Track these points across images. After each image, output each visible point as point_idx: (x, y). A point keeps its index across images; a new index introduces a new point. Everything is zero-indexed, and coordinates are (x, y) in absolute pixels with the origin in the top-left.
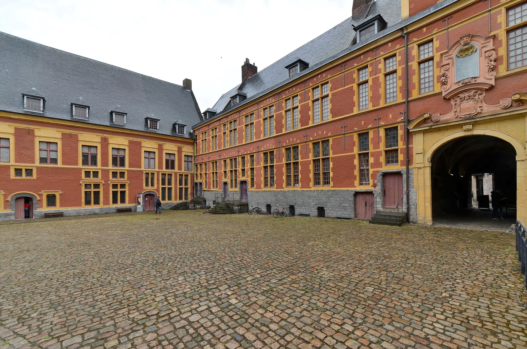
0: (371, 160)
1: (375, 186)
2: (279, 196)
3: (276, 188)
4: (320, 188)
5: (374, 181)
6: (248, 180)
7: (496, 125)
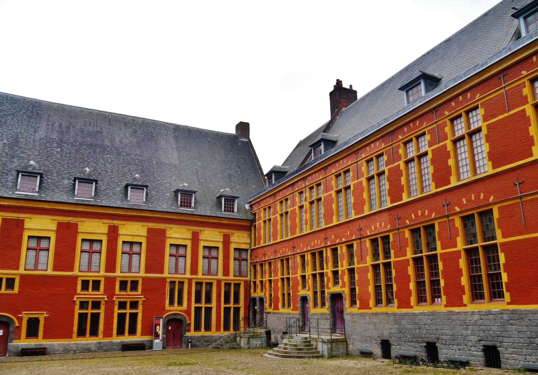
2: (403, 322)
4: (485, 306)
6: (344, 291)
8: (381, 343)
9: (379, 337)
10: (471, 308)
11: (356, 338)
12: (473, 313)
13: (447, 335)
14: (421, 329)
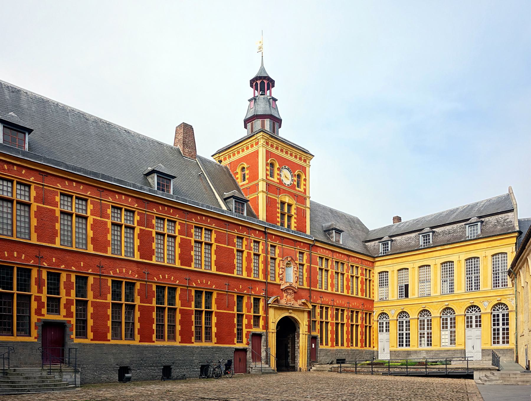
0: (245, 321)
1: (248, 344)
3: (140, 342)
5: (247, 340)
6: (70, 321)
7: (297, 313)
8: (119, 370)
9: (117, 365)
12: (198, 347)
13: (180, 360)
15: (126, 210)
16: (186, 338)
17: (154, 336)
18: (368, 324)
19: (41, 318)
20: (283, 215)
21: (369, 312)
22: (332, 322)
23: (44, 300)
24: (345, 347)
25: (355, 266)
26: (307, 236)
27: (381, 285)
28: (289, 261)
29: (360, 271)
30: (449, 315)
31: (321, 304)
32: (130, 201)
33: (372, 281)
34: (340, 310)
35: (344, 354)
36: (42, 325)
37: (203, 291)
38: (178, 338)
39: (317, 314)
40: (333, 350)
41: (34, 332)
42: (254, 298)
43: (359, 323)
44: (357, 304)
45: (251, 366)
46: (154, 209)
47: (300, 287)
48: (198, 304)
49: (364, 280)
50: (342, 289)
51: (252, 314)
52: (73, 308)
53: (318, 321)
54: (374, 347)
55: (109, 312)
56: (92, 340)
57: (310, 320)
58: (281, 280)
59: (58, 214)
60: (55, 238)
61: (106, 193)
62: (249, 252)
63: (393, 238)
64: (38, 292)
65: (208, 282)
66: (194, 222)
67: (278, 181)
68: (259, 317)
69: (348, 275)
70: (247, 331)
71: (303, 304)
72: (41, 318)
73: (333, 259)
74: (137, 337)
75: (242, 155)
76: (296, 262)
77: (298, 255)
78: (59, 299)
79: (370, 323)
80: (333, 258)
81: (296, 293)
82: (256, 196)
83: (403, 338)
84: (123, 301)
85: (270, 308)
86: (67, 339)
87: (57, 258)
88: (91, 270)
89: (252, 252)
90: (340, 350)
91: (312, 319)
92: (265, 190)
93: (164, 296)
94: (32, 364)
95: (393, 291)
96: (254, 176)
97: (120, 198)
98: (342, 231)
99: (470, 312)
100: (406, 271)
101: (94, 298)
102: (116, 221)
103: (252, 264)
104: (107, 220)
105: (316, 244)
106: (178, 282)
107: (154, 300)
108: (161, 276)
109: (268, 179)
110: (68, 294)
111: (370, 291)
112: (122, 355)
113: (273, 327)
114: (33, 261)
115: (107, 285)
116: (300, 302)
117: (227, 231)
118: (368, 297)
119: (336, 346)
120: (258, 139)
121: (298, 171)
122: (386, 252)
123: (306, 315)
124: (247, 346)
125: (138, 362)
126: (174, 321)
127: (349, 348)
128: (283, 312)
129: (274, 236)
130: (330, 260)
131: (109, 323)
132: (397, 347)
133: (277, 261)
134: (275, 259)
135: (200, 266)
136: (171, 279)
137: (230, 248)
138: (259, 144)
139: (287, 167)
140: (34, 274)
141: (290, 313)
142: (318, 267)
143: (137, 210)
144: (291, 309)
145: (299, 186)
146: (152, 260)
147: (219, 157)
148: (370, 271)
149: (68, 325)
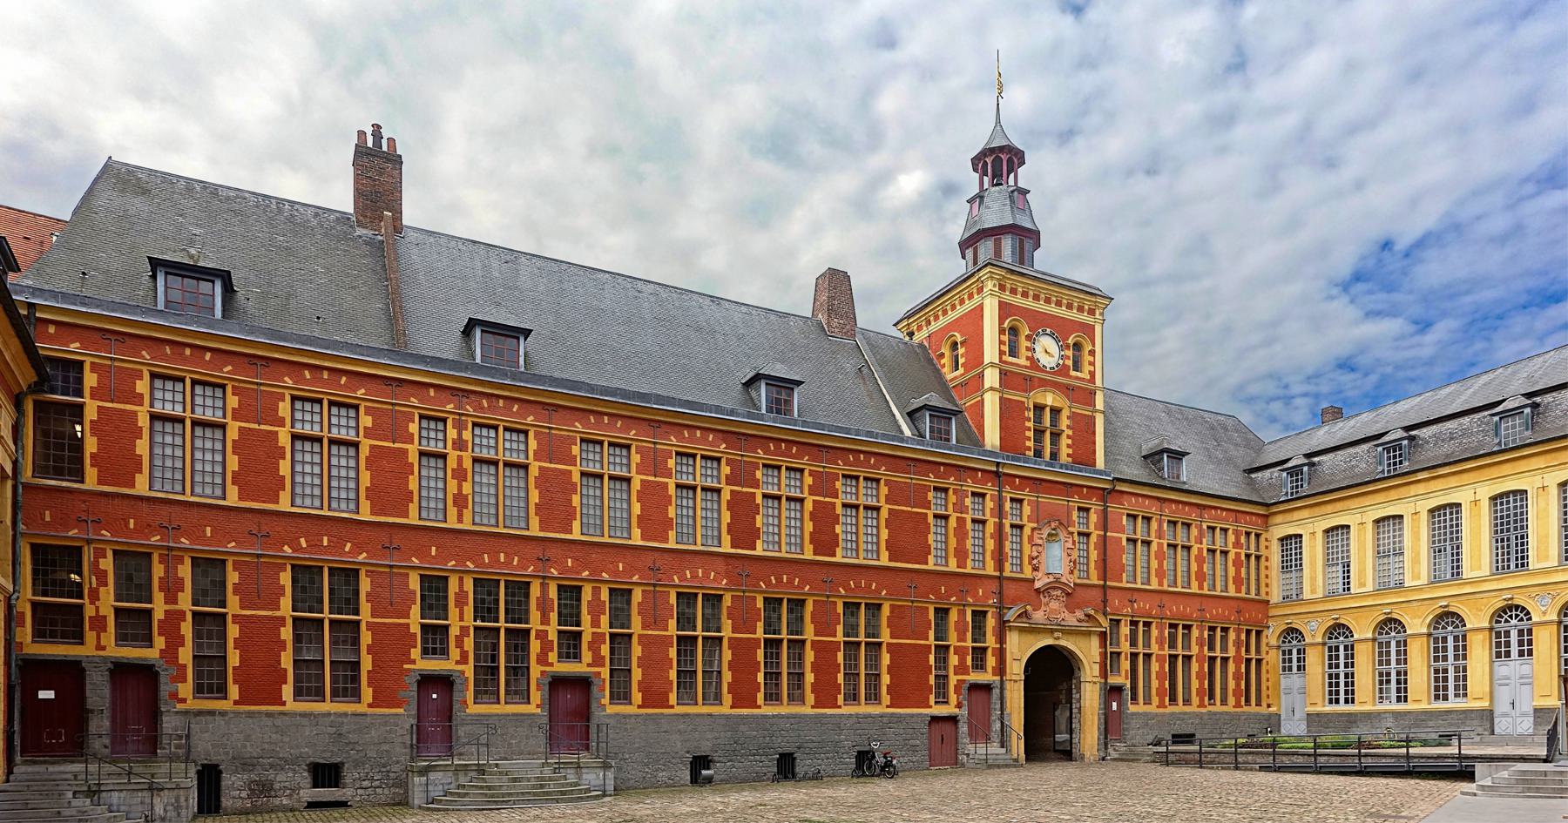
0: (954, 660)
1: (959, 706)
3: (732, 707)
5: (958, 699)
6: (599, 673)
7: (1072, 638)
8: (691, 763)
9: (688, 752)
10: (846, 710)
11: (630, 757)
14: (773, 736)
15: (703, 457)
16: (825, 696)
17: (760, 696)
18: (1253, 655)
19: (548, 669)
20: (1039, 433)
21: (1255, 628)
22: (1160, 653)
23: (553, 636)
24: (1193, 708)
25: (1218, 529)
26: (1100, 472)
27: (1285, 568)
28: (1054, 529)
29: (1231, 538)
30: (1450, 628)
31: (1132, 616)
32: (710, 439)
33: (1263, 559)
34: (1181, 627)
35: (1192, 724)
36: (550, 683)
37: (860, 604)
38: (810, 698)
39: (1122, 639)
40: (1163, 715)
41: (536, 697)
42: (973, 611)
43: (1231, 652)
44: (1223, 612)
45: (966, 752)
46: (759, 451)
47: (1079, 581)
48: (851, 630)
49: (1243, 557)
50: (1186, 579)
51: (969, 644)
52: (605, 650)
53: (1126, 654)
54: (1269, 706)
55: (673, 653)
56: (639, 707)
57: (1106, 653)
58: (1035, 569)
59: (576, 477)
60: (571, 523)
61: (664, 428)
62: (961, 517)
63: (1316, 459)
64: (542, 624)
65: (871, 585)
66: (841, 467)
67: (1028, 364)
68: (985, 649)
69: (1200, 550)
70: (958, 681)
71: (1087, 618)
72: (548, 669)
73: (1163, 517)
74: (727, 698)
75: (952, 316)
76: (1069, 529)
77: (1075, 514)
78: (579, 634)
79: (1258, 651)
80: (1161, 515)
81: (1071, 596)
82: (979, 398)
83: (1337, 685)
84: (699, 632)
85: (1010, 630)
86: (594, 706)
87: (575, 559)
88: (637, 577)
89: (968, 517)
90: (1180, 713)
91: (1109, 650)
92: (997, 386)
93: (780, 618)
94: (532, 754)
95: (1313, 579)
96: (976, 359)
97: (692, 435)
98: (1184, 454)
99: (1503, 620)
100: (1397, 521)
101: (643, 628)
102: (686, 480)
103: (969, 542)
104: (667, 480)
105: (1117, 488)
106: (808, 587)
107: (760, 626)
108: (772, 578)
109: (1005, 362)
110: (596, 623)
111: (1258, 580)
112: (697, 735)
113: (1016, 669)
114: (532, 567)
115: (668, 602)
116: (1080, 614)
117: (911, 479)
118: (1253, 595)
119: (1170, 705)
120: (982, 282)
121: (1076, 337)
122: (1297, 492)
123: (1095, 642)
124: (957, 710)
125: (728, 747)
126: (801, 665)
127: (1203, 710)
128: (1040, 636)
129: (1017, 480)
130: (1154, 519)
131: (673, 675)
132: (1324, 706)
133: (1027, 531)
134: (1021, 527)
135: (854, 553)
136: (794, 584)
137: (918, 513)
138: (985, 290)
139: (1048, 331)
140: (535, 590)
141: (1058, 638)
142: (1124, 537)
143: (725, 456)
144: (1057, 630)
145: (1077, 367)
146: (755, 549)
147: (908, 325)
148: (1258, 536)
149: (595, 681)
